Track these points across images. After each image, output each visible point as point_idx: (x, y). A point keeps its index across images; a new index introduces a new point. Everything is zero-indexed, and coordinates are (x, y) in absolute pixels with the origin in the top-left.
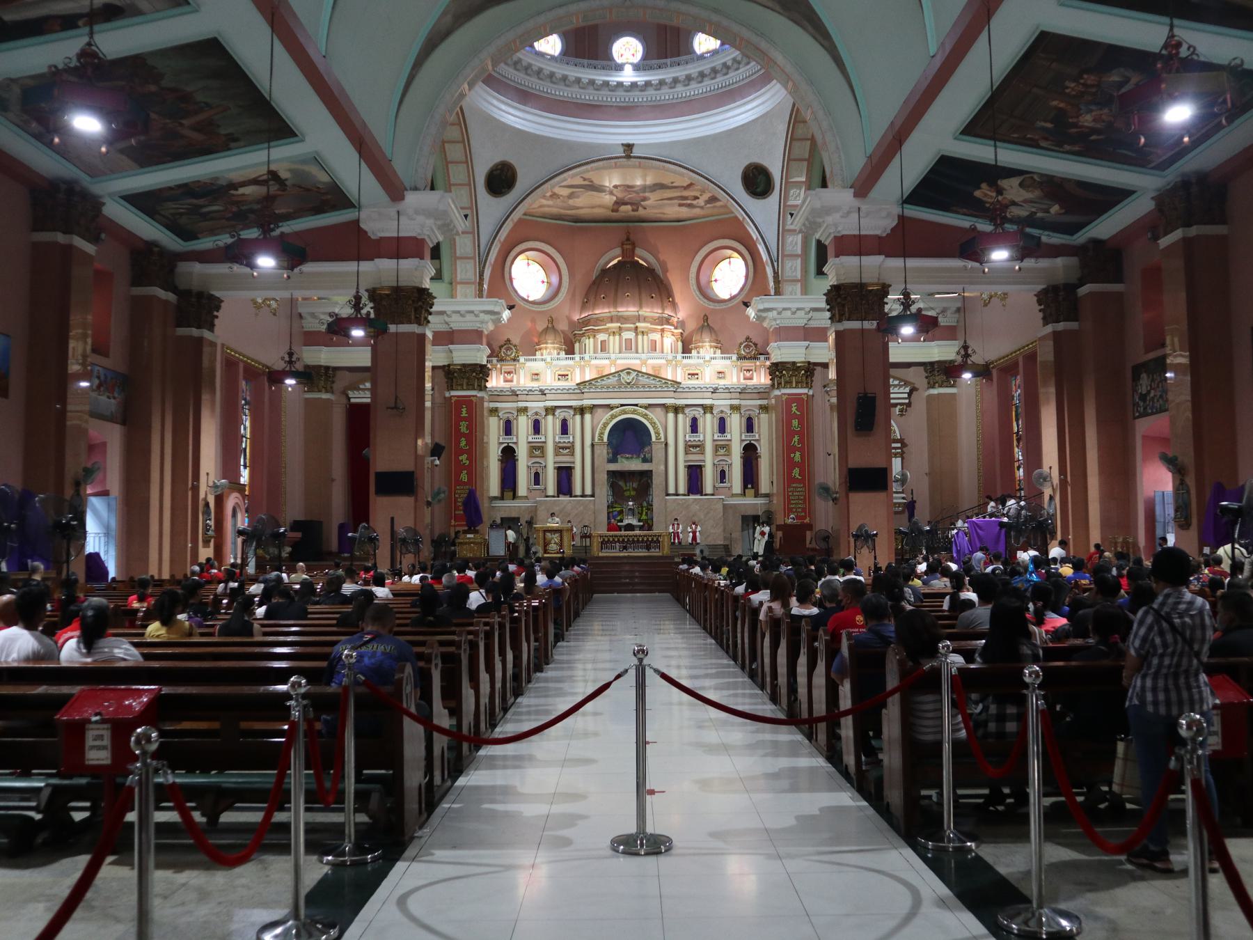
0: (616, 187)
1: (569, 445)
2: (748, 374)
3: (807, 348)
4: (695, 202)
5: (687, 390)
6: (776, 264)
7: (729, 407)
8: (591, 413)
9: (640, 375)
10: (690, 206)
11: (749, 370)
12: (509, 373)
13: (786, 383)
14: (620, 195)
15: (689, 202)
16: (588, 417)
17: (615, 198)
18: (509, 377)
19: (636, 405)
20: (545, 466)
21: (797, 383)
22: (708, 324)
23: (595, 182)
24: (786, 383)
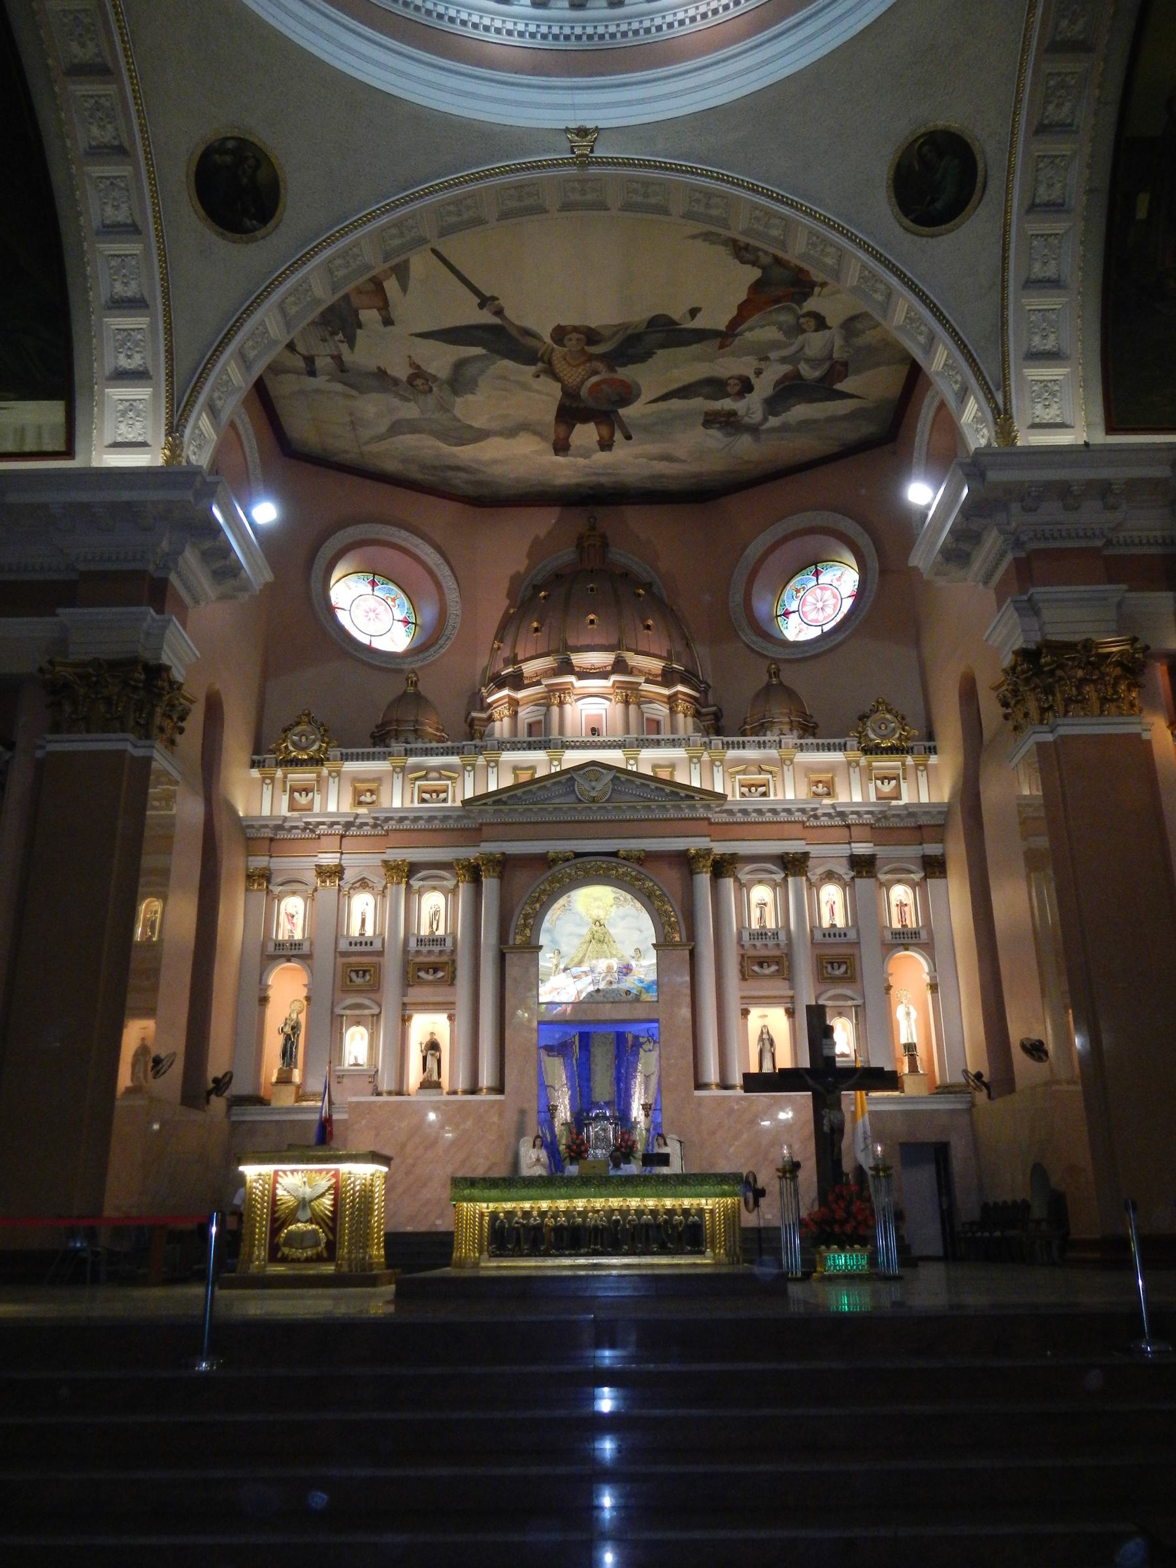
0: (560, 334)
1: (444, 959)
2: (887, 788)
3: (1119, 605)
4: (739, 406)
5: (740, 817)
6: (999, 398)
7: (845, 862)
8: (501, 877)
9: (623, 777)
10: (727, 422)
11: (890, 779)
12: (307, 790)
13: (1068, 701)
14: (572, 375)
15: (726, 404)
16: (490, 885)
17: (554, 391)
18: (303, 800)
19: (614, 854)
20: (378, 1015)
21: (1104, 700)
22: (781, 683)
23: (507, 313)
24: (1068, 701)
